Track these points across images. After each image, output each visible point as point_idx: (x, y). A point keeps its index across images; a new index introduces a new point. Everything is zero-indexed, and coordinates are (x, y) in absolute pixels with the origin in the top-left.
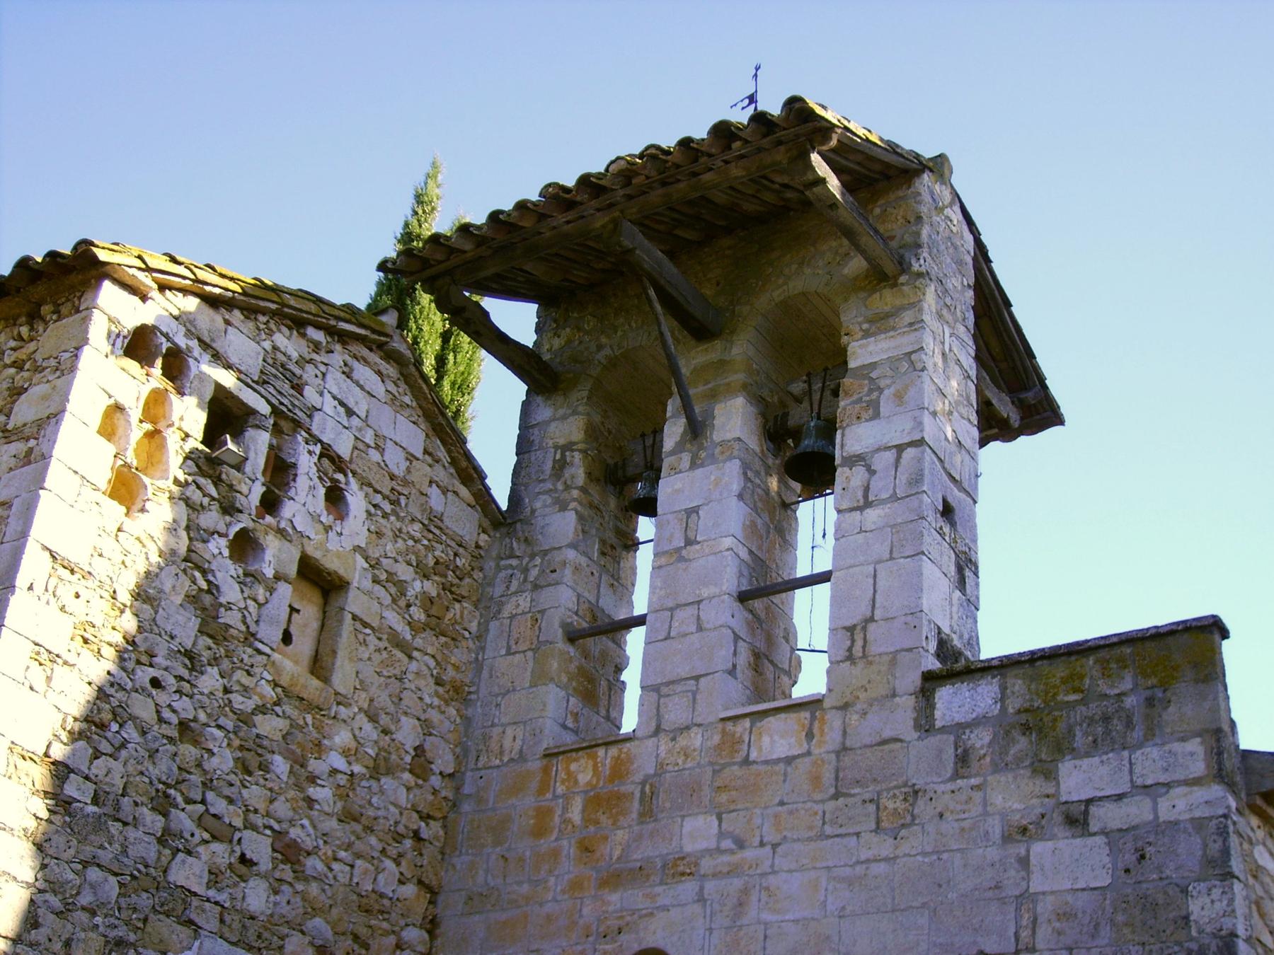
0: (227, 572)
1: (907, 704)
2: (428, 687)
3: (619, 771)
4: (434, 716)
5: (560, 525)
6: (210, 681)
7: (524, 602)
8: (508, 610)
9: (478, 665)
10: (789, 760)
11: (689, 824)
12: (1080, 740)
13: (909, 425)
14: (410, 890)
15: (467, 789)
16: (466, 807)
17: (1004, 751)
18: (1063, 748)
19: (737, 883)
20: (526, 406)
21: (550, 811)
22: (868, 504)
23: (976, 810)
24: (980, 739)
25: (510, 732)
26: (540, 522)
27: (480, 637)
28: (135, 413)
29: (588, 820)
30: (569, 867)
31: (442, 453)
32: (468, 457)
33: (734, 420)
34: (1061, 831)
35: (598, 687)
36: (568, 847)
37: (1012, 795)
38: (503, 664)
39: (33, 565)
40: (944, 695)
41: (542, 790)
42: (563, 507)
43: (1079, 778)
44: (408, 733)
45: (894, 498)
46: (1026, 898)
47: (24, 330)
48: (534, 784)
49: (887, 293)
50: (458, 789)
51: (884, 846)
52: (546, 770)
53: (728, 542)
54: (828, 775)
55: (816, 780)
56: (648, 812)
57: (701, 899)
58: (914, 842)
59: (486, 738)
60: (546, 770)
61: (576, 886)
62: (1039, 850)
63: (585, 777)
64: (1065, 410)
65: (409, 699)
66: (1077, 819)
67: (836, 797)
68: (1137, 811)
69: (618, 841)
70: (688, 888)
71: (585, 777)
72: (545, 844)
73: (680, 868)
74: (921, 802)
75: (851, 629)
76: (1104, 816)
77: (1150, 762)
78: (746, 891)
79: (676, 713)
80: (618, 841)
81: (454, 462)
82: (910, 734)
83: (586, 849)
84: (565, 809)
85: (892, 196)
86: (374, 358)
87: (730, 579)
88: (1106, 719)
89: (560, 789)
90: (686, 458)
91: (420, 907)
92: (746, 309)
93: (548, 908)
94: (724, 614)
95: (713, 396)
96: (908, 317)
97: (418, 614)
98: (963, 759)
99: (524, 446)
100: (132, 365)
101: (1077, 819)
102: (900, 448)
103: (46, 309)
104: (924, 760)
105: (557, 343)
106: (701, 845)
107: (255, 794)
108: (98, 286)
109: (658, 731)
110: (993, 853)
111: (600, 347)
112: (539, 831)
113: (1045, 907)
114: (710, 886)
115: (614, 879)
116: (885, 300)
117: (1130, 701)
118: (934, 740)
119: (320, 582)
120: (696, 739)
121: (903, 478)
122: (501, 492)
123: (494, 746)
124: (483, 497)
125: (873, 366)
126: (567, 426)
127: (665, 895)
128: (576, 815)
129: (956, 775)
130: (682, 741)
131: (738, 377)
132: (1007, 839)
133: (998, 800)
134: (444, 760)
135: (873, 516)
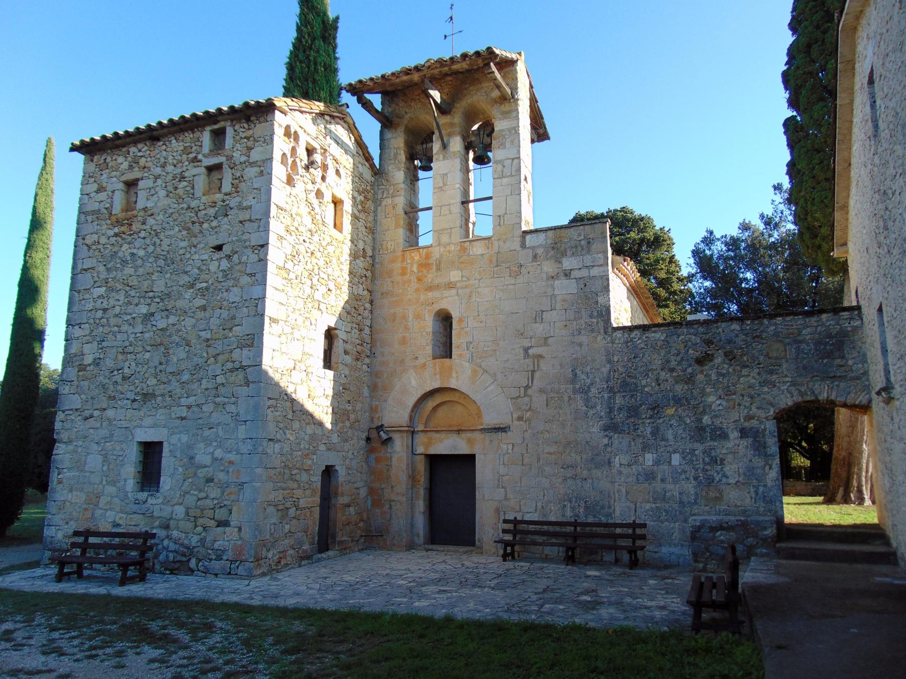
0: (315, 202)
1: (518, 240)
2: (364, 229)
3: (428, 256)
4: (366, 239)
5: (399, 176)
6: (316, 238)
7: (389, 201)
8: (384, 203)
9: (375, 221)
10: (482, 255)
11: (452, 273)
12: (569, 253)
13: (515, 152)
14: (366, 292)
15: (377, 260)
16: (377, 266)
17: (547, 254)
18: (564, 254)
19: (468, 290)
20: (382, 133)
21: (406, 268)
22: (503, 177)
23: (539, 271)
24: (540, 251)
25: (389, 243)
26: (391, 174)
27: (375, 212)
28: (289, 156)
30: (414, 285)
31: (361, 153)
32: (368, 153)
33: (456, 144)
34: (563, 278)
35: (412, 228)
36: (414, 278)
37: (549, 267)
39: (273, 210)
40: (528, 237)
41: (403, 261)
42: (399, 170)
43: (568, 263)
44: (361, 245)
45: (511, 175)
46: (553, 296)
47: (246, 125)
48: (400, 259)
49: (507, 105)
50: (373, 261)
51: (513, 281)
52: (403, 255)
53: (458, 186)
54: (494, 260)
55: (491, 261)
56: (438, 269)
57: (458, 295)
58: (520, 279)
59: (382, 245)
60: (403, 255)
61: (417, 290)
62: (557, 283)
63: (417, 258)
64: (550, 135)
65: (360, 235)
66: (567, 274)
67: (497, 266)
68: (584, 273)
69: (431, 277)
70: (454, 292)
71: (417, 258)
72: (406, 278)
73: (450, 286)
74: (523, 268)
75: (499, 216)
78: (471, 292)
79: (445, 239)
80: (431, 277)
81: (364, 154)
82: (518, 248)
83: (419, 280)
84: (412, 267)
85: (507, 69)
86: (342, 122)
87: (459, 199)
88: (576, 247)
89: (409, 261)
90: (441, 156)
91: (368, 297)
92: (458, 105)
93: (409, 297)
94: (457, 208)
95: (450, 135)
96: (514, 114)
97: (360, 207)
98: (535, 257)
99: (382, 147)
100: (286, 139)
101: (567, 274)
102: (513, 159)
103: (252, 118)
104: (524, 257)
105: (390, 110)
106: (457, 279)
107: (330, 271)
108: (273, 113)
109: (439, 245)
110: (544, 283)
111: (406, 113)
112: (403, 274)
113: (559, 298)
114: (460, 291)
115: (430, 289)
116: (506, 107)
117: (583, 243)
118: (526, 251)
119: (337, 202)
120: (452, 248)
121: (514, 169)
122: (377, 162)
123: (384, 247)
124: (372, 166)
125: (503, 130)
126: (398, 141)
127: (446, 293)
128: (415, 269)
129: (533, 261)
130: (448, 248)
131: (458, 129)
132: (547, 279)
133: (545, 268)
134: (369, 253)
135: (505, 180)
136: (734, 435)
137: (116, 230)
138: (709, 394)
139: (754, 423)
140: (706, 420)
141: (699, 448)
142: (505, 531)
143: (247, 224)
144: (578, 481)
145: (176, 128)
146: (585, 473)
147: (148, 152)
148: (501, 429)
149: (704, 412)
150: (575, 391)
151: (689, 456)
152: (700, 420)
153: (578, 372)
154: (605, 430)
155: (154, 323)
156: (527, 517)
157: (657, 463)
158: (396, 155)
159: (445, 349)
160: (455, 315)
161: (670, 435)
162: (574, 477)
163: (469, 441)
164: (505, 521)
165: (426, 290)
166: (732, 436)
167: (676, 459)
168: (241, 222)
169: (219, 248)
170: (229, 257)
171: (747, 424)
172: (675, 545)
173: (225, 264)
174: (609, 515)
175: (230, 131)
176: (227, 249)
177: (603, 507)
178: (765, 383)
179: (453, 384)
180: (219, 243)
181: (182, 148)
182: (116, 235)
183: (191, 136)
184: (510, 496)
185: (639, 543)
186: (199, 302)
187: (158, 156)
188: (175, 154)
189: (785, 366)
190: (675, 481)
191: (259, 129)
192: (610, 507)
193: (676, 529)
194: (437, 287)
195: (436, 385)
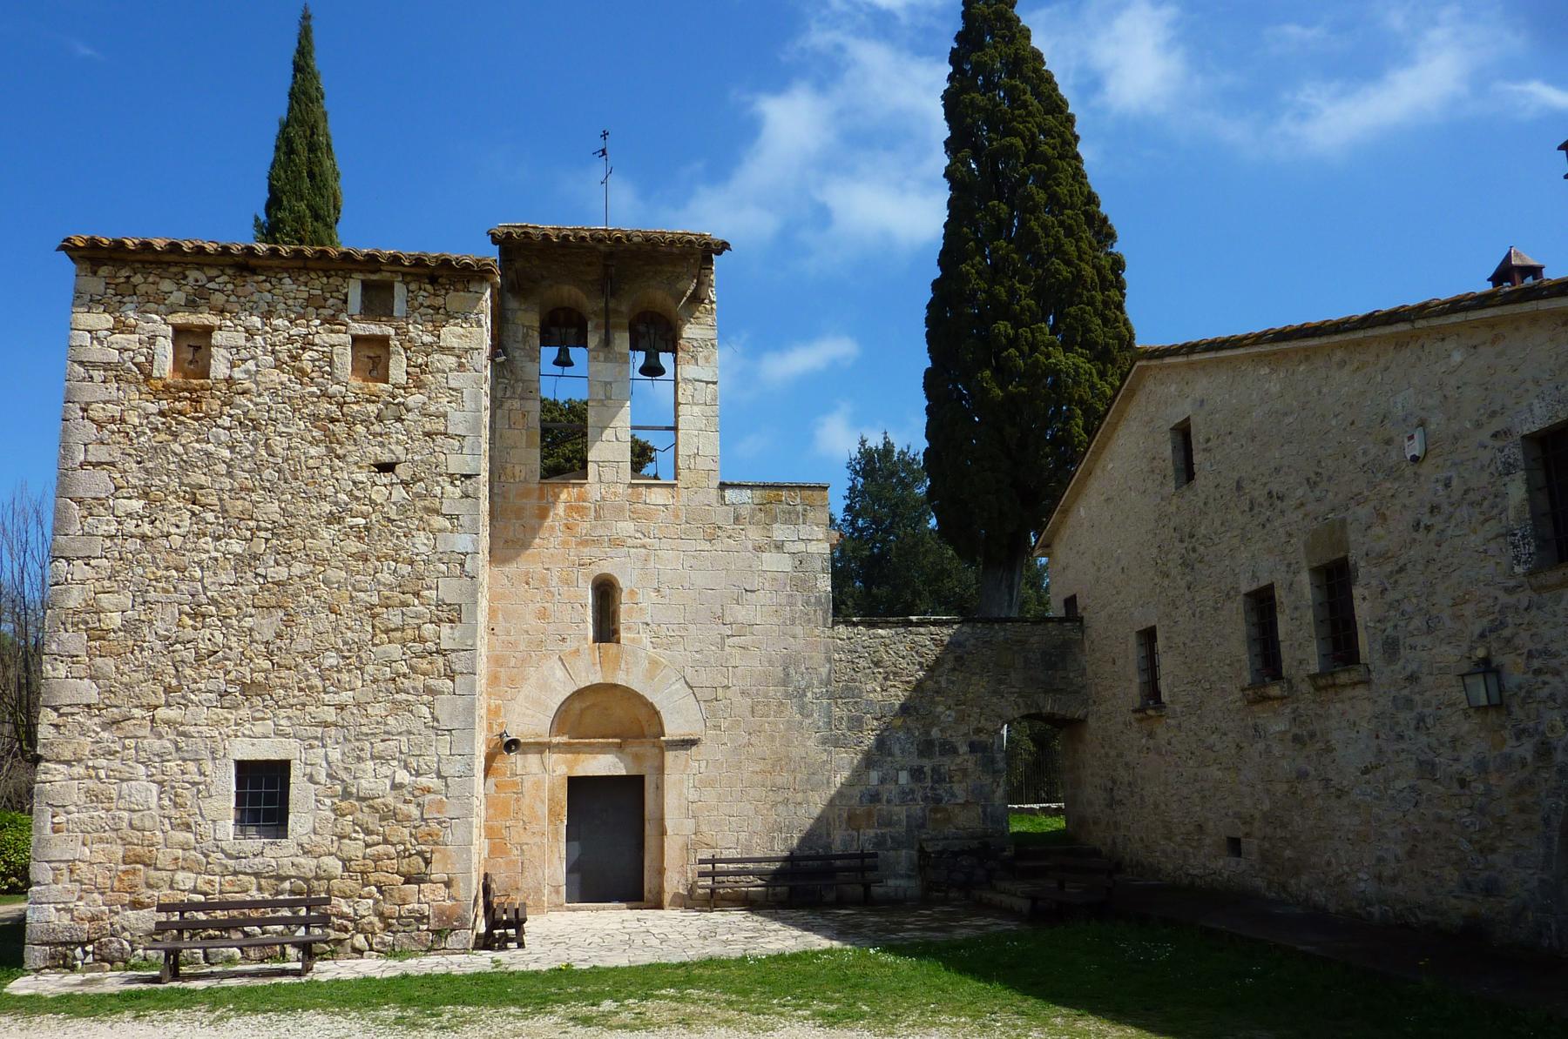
7: (516, 404)
8: (507, 405)
11: (620, 524)
25: (517, 468)
29: (568, 515)
37: (754, 534)
38: (507, 433)
48: (536, 494)
51: (707, 546)
59: (504, 469)
68: (801, 547)
73: (616, 543)
76: (789, 547)
77: (804, 531)
101: (779, 547)
104: (721, 516)
123: (508, 471)
131: (626, 322)
136: (963, 749)
137: (164, 405)
138: (938, 704)
139: (984, 737)
140: (935, 733)
141: (927, 765)
142: (702, 874)
143: (439, 439)
144: (791, 806)
145: (300, 263)
146: (800, 797)
147: (230, 286)
148: (688, 743)
149: (932, 725)
150: (787, 695)
151: (916, 774)
152: (928, 733)
153: (792, 671)
154: (824, 743)
155: (261, 571)
156: (726, 854)
157: (882, 781)
158: (526, 336)
159: (606, 628)
160: (623, 582)
161: (896, 750)
162: (786, 802)
163: (637, 758)
164: (702, 862)
165: (578, 544)
166: (961, 751)
167: (904, 778)
168: (428, 434)
169: (386, 468)
170: (405, 484)
171: (975, 738)
172: (902, 877)
173: (399, 493)
174: (828, 846)
175: (400, 290)
176: (403, 472)
177: (820, 836)
178: (995, 692)
179: (621, 679)
180: (386, 458)
181: (305, 295)
182: (162, 413)
183: (325, 280)
184: (704, 828)
185: (870, 875)
186: (354, 546)
187: (255, 298)
188: (290, 302)
189: (1013, 674)
190: (903, 802)
191: (454, 299)
192: (829, 835)
193: (904, 857)
194: (596, 542)
195: (597, 679)
